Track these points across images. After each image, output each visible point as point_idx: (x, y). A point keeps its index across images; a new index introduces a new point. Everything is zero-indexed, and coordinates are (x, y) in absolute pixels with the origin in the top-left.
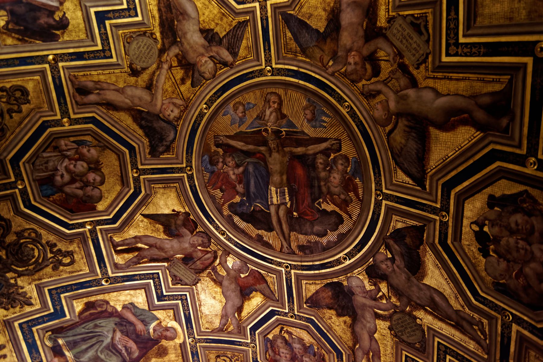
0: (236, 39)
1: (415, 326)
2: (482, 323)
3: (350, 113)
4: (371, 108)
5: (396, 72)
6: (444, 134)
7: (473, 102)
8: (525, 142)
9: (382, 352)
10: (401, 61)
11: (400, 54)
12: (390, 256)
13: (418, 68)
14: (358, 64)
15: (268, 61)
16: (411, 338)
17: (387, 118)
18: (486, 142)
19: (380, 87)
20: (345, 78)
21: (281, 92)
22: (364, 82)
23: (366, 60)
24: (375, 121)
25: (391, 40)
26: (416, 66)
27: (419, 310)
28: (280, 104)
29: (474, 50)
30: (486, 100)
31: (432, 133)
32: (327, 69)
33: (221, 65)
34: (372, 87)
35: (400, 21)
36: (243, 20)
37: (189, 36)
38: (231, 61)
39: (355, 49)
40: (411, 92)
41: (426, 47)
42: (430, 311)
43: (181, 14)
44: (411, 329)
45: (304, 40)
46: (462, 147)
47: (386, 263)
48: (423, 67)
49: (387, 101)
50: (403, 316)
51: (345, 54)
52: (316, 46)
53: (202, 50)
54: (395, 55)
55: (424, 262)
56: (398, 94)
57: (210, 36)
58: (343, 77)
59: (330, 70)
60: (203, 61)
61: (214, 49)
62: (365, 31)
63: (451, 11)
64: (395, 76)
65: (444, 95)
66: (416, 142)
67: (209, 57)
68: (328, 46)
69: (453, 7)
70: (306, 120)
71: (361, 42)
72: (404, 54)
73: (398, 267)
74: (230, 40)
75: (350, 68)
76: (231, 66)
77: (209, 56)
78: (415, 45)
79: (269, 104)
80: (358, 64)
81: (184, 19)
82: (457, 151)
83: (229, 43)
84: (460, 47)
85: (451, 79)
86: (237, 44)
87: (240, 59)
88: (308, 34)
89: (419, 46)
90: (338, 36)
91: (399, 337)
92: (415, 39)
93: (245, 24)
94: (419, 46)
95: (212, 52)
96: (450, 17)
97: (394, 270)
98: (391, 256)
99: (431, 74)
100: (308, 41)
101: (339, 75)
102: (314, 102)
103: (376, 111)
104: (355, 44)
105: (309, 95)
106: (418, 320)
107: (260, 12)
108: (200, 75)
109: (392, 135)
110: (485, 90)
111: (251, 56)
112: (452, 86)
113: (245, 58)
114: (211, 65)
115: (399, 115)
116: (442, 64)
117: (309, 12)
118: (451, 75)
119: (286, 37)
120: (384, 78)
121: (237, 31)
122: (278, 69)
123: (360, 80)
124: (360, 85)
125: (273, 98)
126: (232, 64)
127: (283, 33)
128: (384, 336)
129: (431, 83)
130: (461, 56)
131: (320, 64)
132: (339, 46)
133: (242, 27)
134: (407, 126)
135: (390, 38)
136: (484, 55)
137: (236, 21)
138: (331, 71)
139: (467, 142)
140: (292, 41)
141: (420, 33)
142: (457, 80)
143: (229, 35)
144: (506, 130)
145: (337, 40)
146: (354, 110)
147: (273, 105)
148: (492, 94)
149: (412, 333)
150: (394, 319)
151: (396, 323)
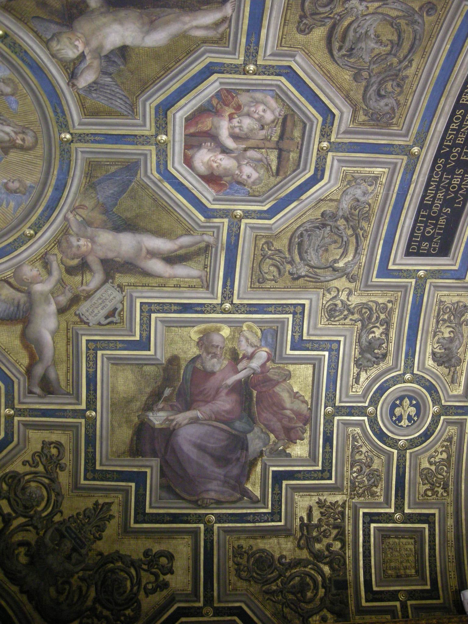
0: (110, 97)
3: (23, 236)
4: (32, 263)
5: (71, 292)
6: (19, 339)
7: (50, 363)
8: (24, 407)
10: (82, 297)
11: (89, 296)
13: (76, 314)
14: (78, 250)
15: (79, 138)
17: (23, 280)
18: (19, 376)
19: (56, 274)
20: (63, 233)
21: (40, 151)
22: (60, 256)
23: (82, 259)
24: (18, 267)
25: (102, 288)
26: (77, 312)
28: (22, 148)
29: (91, 363)
30: (52, 375)
31: (16, 326)
32: (71, 212)
33: (72, 69)
34: (55, 265)
35: (119, 297)
36: (135, 110)
37: (116, 27)
38: (78, 85)
39: (94, 247)
40: (53, 308)
41: (94, 322)
43: (152, 22)
45: (106, 187)
46: (9, 354)
48: (77, 319)
49: (41, 282)
51: (89, 235)
52: (98, 201)
53: (94, 44)
54: (87, 292)
56: (50, 295)
57: (116, 60)
58: (63, 231)
59: (71, 216)
60: (77, 43)
61: (96, 63)
62: (112, 260)
63: (123, 343)
64: (67, 291)
65: (53, 339)
66: (5, 311)
67: (83, 52)
68: (97, 216)
69: (125, 346)
70: (5, 181)
71: (101, 255)
72: (88, 301)
74: (109, 88)
75: (73, 240)
76: (70, 84)
77: (86, 53)
78: (96, 311)
79: (20, 133)
80: (78, 250)
81: (143, 24)
82: (4, 350)
83: (104, 85)
84: (94, 352)
85: (68, 344)
86: (102, 97)
87: (81, 98)
88: (112, 193)
89: (96, 315)
90: (107, 229)
92: (102, 312)
93: (130, 112)
94: (96, 315)
95: (91, 59)
96: (118, 343)
99: (71, 327)
100: (104, 192)
101: (66, 227)
102: (30, 193)
103: (30, 268)
104: (99, 248)
105: (39, 187)
107: (143, 136)
108: (54, 35)
109: (7, 286)
110: (59, 373)
111: (85, 115)
112: (62, 345)
113: (83, 105)
114: (71, 54)
115: (29, 294)
116: (80, 336)
117: (137, 197)
118: (71, 345)
119: (110, 165)
120: (65, 280)
121: (121, 99)
122: (69, 151)
123: (62, 252)
124: (56, 251)
125: (29, 140)
126: (74, 85)
127: (115, 162)
129: (64, 325)
130: (87, 353)
131: (77, 204)
132: (97, 229)
133: (126, 107)
134: (19, 302)
135: (105, 285)
136: (87, 372)
137: (135, 100)
138: (69, 217)
139: (15, 359)
140: (105, 173)
141: (107, 317)
142: (67, 350)
143: (116, 86)
144: (30, 392)
145: (104, 226)
146: (27, 242)
147: (18, 137)
148: (58, 379)
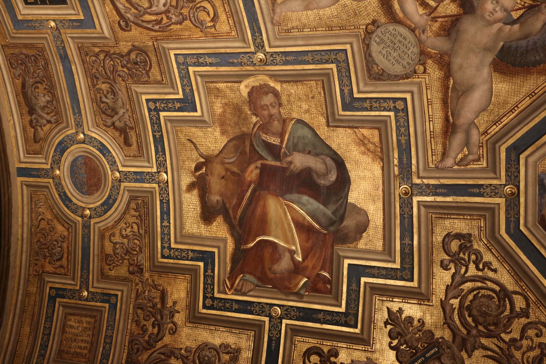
1: (409, 64)
2: (479, 160)
9: (321, 12)
12: (515, 15)
16: (381, 57)
27: (441, 70)
42: (448, 85)
44: (398, 58)
47: (497, 9)
50: (414, 43)
55: (531, 73)
73: (500, 30)
91: (370, 38)
97: (490, 24)
98: (516, 18)
106: (422, 68)
128: (356, 15)
149: (391, 59)
150: (396, 28)
151: (393, 32)
